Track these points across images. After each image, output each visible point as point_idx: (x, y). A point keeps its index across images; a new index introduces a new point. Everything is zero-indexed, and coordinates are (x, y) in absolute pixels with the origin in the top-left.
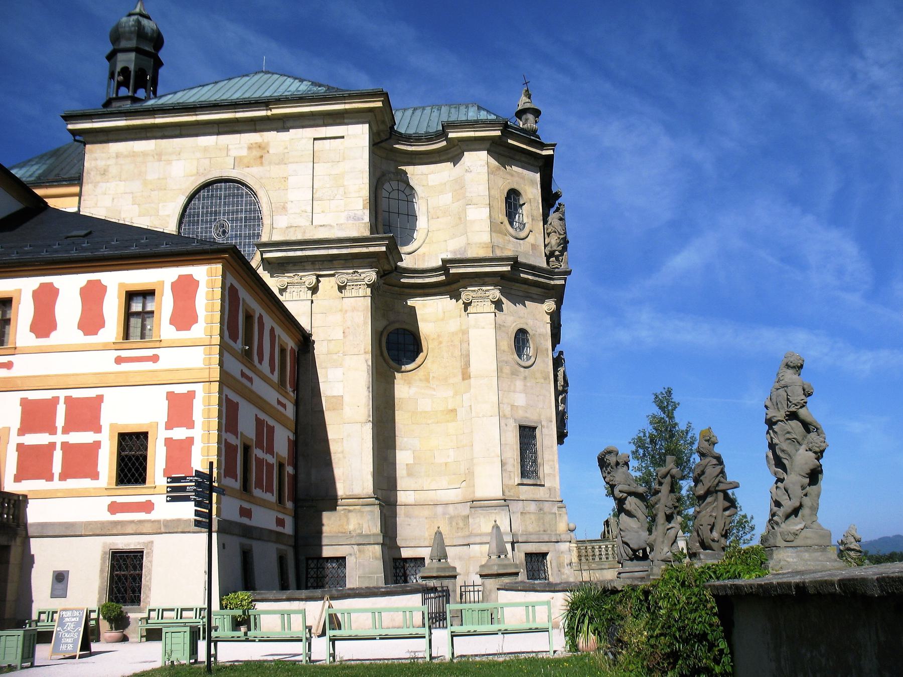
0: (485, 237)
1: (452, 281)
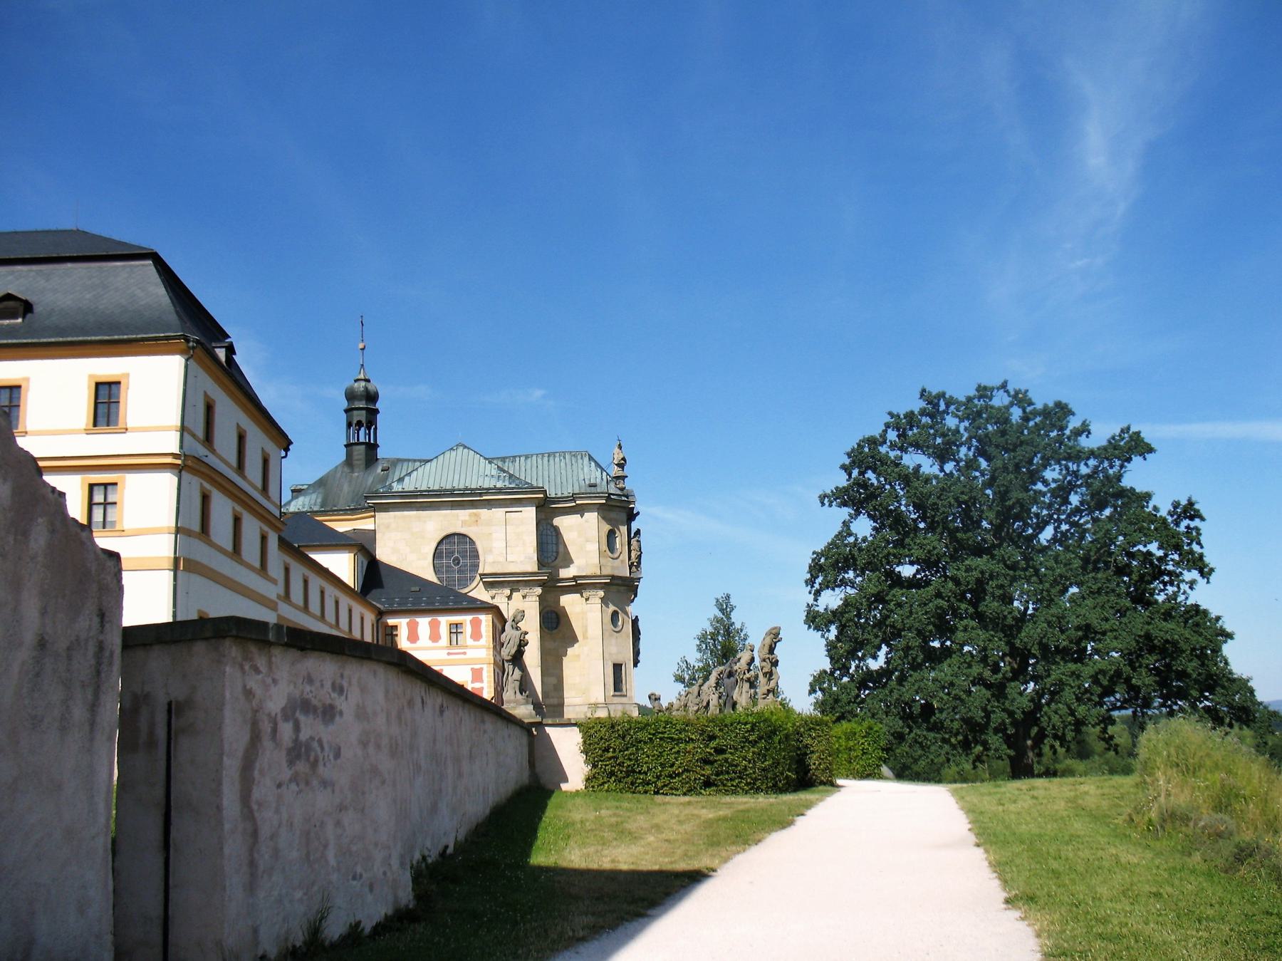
1: (578, 586)
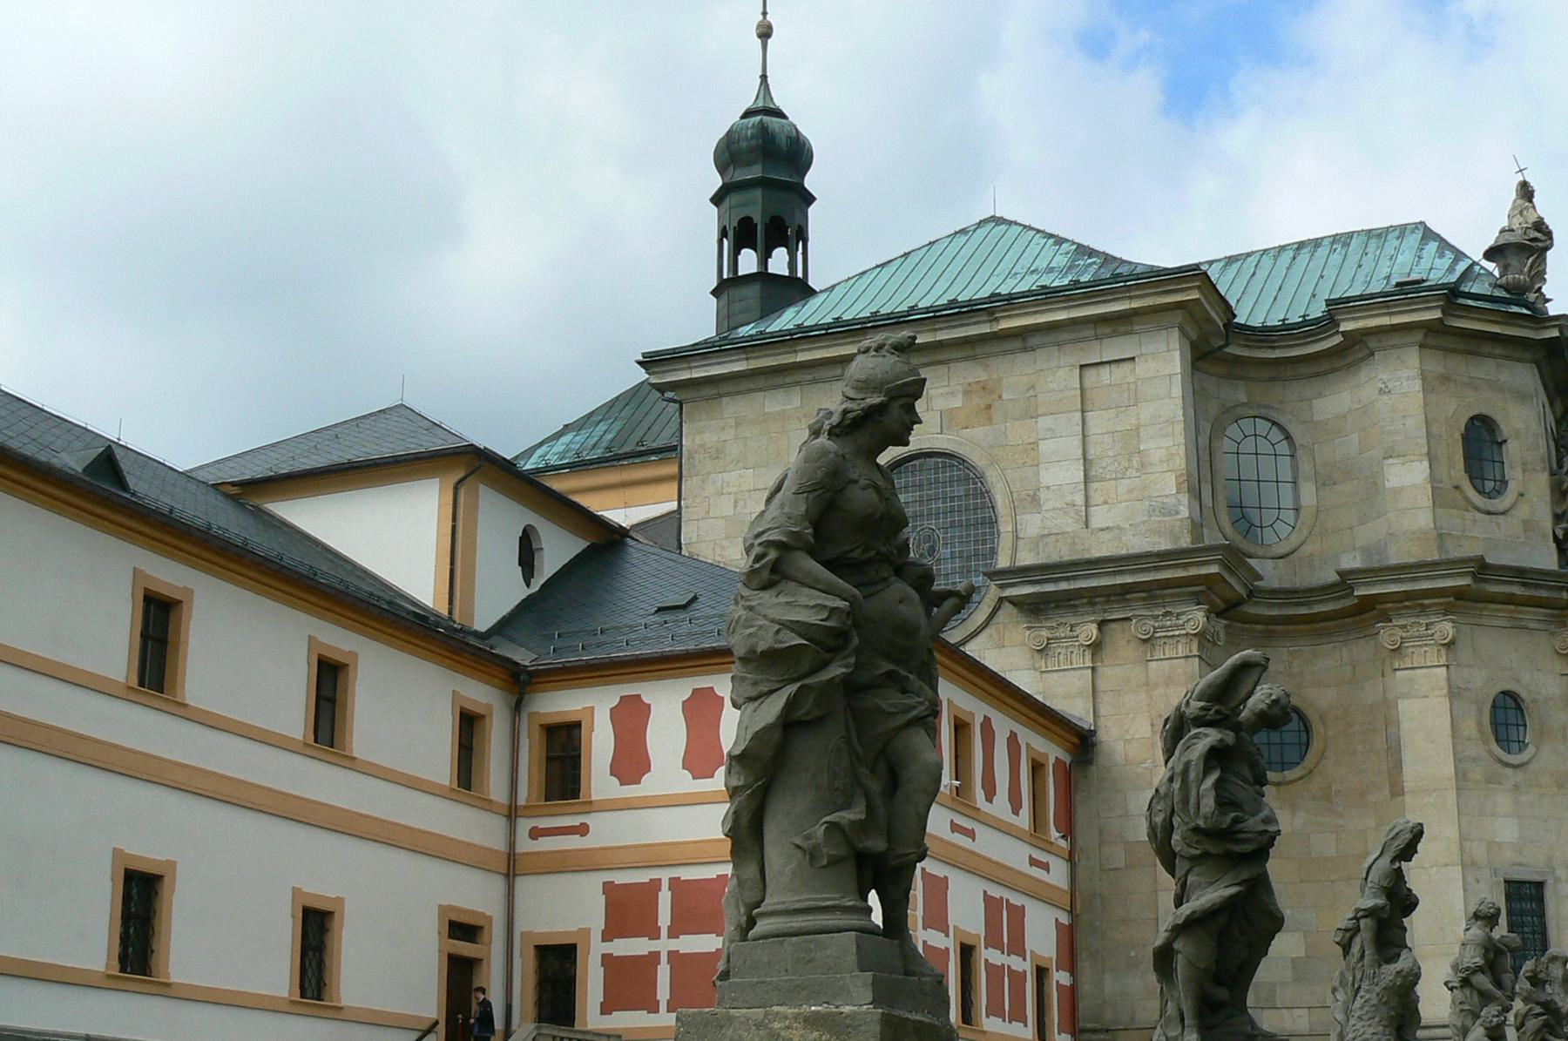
0: (1423, 519)
